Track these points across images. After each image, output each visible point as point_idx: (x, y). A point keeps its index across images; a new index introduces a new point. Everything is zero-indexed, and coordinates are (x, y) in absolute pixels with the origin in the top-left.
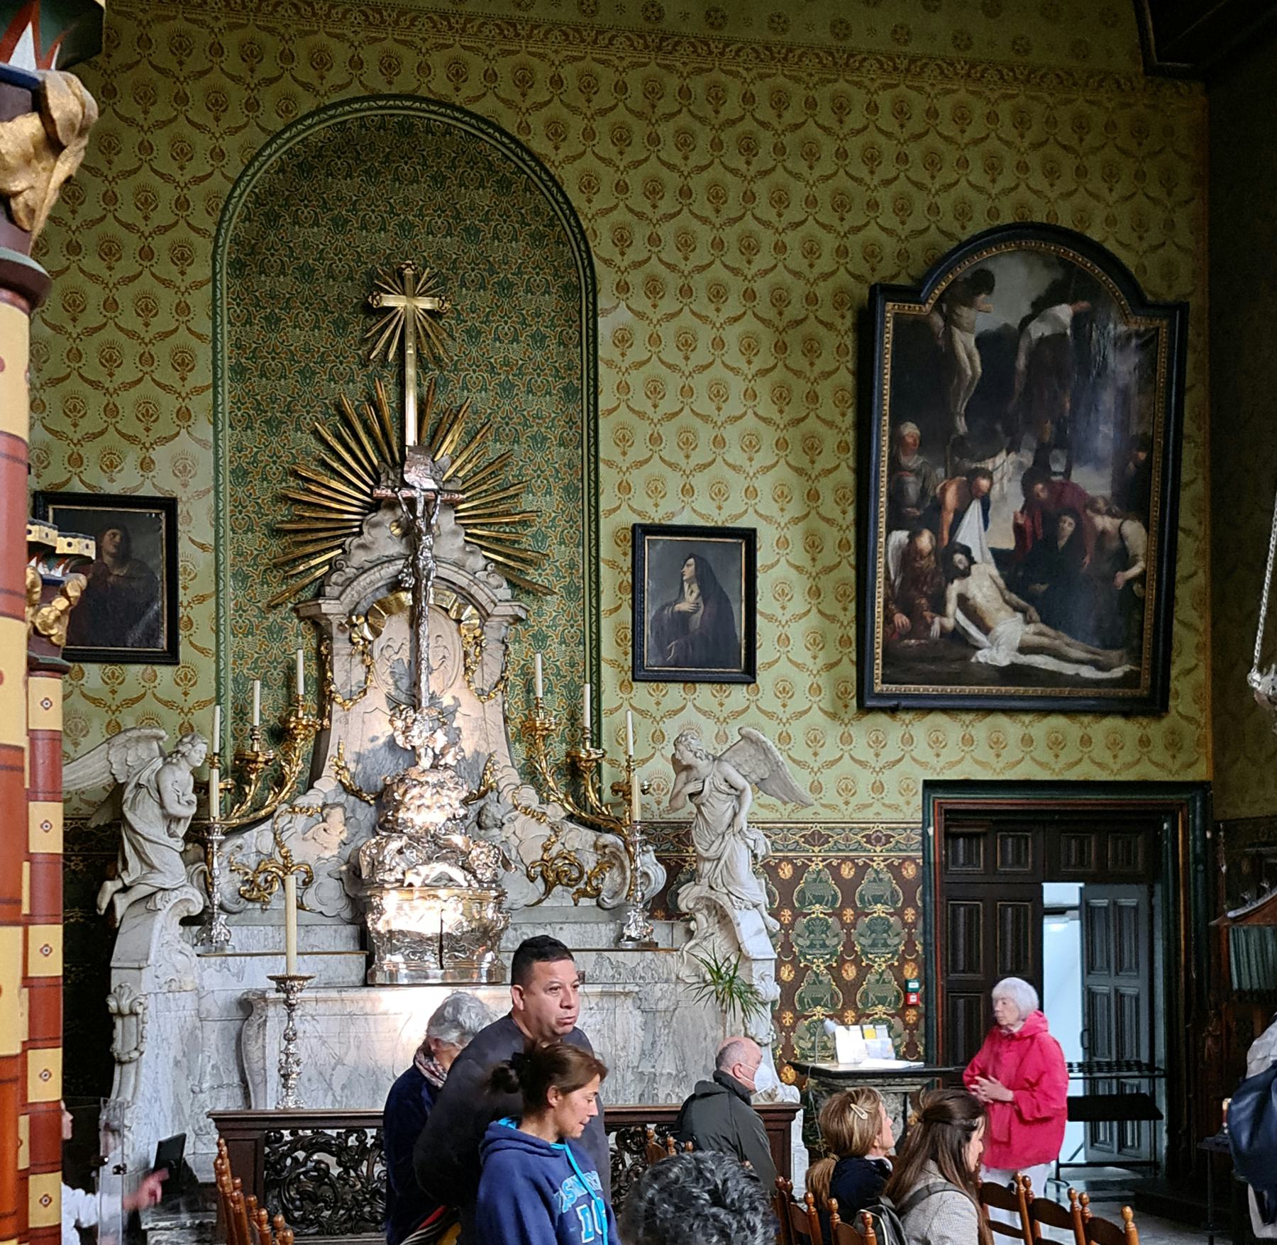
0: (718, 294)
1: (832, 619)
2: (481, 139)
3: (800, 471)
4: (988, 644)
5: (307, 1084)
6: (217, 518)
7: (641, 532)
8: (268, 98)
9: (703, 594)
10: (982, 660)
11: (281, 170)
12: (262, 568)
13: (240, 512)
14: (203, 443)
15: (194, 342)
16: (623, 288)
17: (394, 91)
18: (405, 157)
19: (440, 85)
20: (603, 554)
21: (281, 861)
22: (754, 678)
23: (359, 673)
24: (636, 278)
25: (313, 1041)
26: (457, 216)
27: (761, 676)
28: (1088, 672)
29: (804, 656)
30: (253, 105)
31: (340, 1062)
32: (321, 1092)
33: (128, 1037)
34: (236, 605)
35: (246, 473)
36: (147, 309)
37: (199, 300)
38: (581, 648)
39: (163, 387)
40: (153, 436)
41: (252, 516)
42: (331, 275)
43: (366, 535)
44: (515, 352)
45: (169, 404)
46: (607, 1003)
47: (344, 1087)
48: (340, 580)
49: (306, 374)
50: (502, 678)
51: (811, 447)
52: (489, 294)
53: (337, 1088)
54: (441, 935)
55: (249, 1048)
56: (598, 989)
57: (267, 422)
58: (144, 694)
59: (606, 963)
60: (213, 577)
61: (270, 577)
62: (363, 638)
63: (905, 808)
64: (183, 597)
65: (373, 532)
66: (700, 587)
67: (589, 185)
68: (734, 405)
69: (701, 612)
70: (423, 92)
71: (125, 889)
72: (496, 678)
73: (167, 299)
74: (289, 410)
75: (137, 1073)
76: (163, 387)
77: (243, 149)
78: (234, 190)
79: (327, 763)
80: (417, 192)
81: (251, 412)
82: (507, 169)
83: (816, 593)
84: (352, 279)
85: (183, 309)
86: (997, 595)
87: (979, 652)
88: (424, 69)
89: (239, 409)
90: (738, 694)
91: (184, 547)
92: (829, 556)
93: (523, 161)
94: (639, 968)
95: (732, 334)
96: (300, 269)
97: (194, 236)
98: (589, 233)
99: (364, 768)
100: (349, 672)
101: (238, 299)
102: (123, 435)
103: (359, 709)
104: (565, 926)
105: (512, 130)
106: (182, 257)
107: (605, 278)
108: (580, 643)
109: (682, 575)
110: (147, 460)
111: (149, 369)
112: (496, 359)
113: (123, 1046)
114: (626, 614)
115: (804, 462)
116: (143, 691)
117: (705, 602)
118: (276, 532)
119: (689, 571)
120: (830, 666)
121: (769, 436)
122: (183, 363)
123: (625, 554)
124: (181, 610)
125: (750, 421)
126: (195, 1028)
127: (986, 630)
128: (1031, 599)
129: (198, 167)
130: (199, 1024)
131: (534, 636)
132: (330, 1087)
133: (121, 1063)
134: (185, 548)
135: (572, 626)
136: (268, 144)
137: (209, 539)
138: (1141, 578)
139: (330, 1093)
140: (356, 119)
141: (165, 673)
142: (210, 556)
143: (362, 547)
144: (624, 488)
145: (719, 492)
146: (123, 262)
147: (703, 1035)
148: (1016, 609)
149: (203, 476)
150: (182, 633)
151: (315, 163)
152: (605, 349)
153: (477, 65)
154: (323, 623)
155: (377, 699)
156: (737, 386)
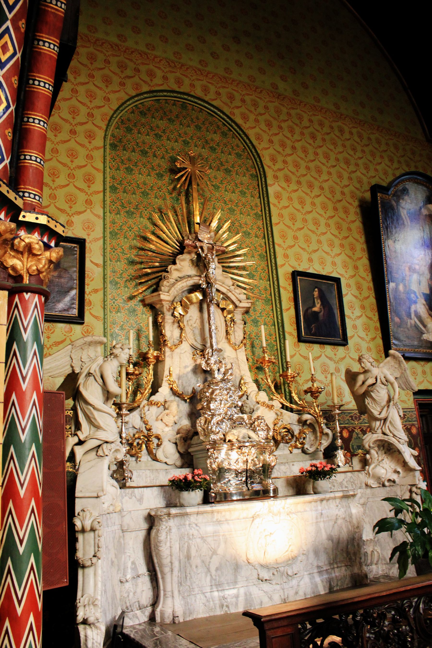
0: (311, 186)
1: (370, 318)
2: (214, 116)
3: (349, 257)
4: (426, 332)
5: (195, 569)
6: (104, 252)
7: (295, 274)
8: (129, 83)
9: (322, 304)
10: (425, 338)
11: (133, 112)
12: (125, 279)
13: (114, 252)
14: (98, 216)
15: (94, 172)
16: (276, 177)
17: (181, 90)
18: (185, 117)
19: (199, 92)
20: (281, 284)
21: (146, 432)
22: (347, 342)
23: (177, 332)
24: (280, 174)
25: (199, 540)
26: (207, 142)
27: (350, 342)
29: (363, 334)
30: (122, 84)
31: (215, 553)
32: (203, 575)
33: (87, 548)
34: (112, 296)
35: (116, 234)
36: (73, 155)
37: (98, 155)
38: (273, 327)
39: (79, 189)
40: (73, 210)
41: (120, 254)
42: (155, 156)
43: (178, 264)
44: (234, 197)
45: (81, 197)
46: (345, 502)
47: (217, 569)
48: (168, 284)
49: (145, 194)
50: (244, 338)
51: (353, 249)
52: (222, 173)
53: (213, 569)
54: (247, 470)
55: (161, 549)
56: (341, 494)
57: (127, 212)
58: (65, 339)
60: (102, 281)
61: (128, 284)
62: (180, 314)
63: (408, 402)
64: (87, 290)
65: (182, 263)
66: (321, 301)
67: (259, 138)
68: (323, 229)
69: (323, 312)
70: (192, 93)
72: (242, 338)
73: (82, 152)
74: (137, 208)
75: (95, 574)
76: (79, 189)
77: (118, 99)
78: (113, 114)
79: (165, 379)
80: (190, 130)
81: (119, 207)
82: (225, 129)
83: (363, 307)
84: (164, 158)
85: (89, 157)
86: (426, 312)
87: (424, 335)
88: (192, 86)
89: (114, 205)
90: (341, 349)
91: (88, 265)
92: (366, 293)
93: (232, 126)
94: (344, 482)
95: (318, 201)
96: (141, 151)
97: (96, 129)
98: (261, 155)
99: (182, 383)
100: (172, 331)
101: (113, 159)
102: (58, 209)
103: (177, 351)
104: (295, 463)
105: (228, 113)
106: (90, 136)
107: (270, 174)
108: (272, 325)
109: (314, 295)
110: (70, 221)
111: (72, 181)
112: (227, 198)
113: (84, 555)
114: (292, 311)
115: (350, 254)
116: (65, 337)
117: (324, 309)
118: (132, 263)
119: (316, 293)
120: (373, 339)
121: (337, 242)
122: (89, 180)
123: (289, 285)
124: (86, 296)
125: (329, 235)
126: (120, 537)
127: (425, 326)
129: (98, 102)
130: (121, 534)
131: (253, 321)
132: (209, 570)
133: (84, 567)
135: (268, 317)
136: (128, 100)
137: (101, 262)
139: (209, 575)
140: (164, 99)
141: (77, 328)
142: (101, 270)
143: (177, 270)
144: (286, 256)
145: (322, 263)
146: (61, 134)
149: (98, 231)
150: (86, 308)
151: (147, 112)
152: (272, 199)
153: (213, 89)
154: (158, 306)
155: (185, 347)
156: (323, 221)
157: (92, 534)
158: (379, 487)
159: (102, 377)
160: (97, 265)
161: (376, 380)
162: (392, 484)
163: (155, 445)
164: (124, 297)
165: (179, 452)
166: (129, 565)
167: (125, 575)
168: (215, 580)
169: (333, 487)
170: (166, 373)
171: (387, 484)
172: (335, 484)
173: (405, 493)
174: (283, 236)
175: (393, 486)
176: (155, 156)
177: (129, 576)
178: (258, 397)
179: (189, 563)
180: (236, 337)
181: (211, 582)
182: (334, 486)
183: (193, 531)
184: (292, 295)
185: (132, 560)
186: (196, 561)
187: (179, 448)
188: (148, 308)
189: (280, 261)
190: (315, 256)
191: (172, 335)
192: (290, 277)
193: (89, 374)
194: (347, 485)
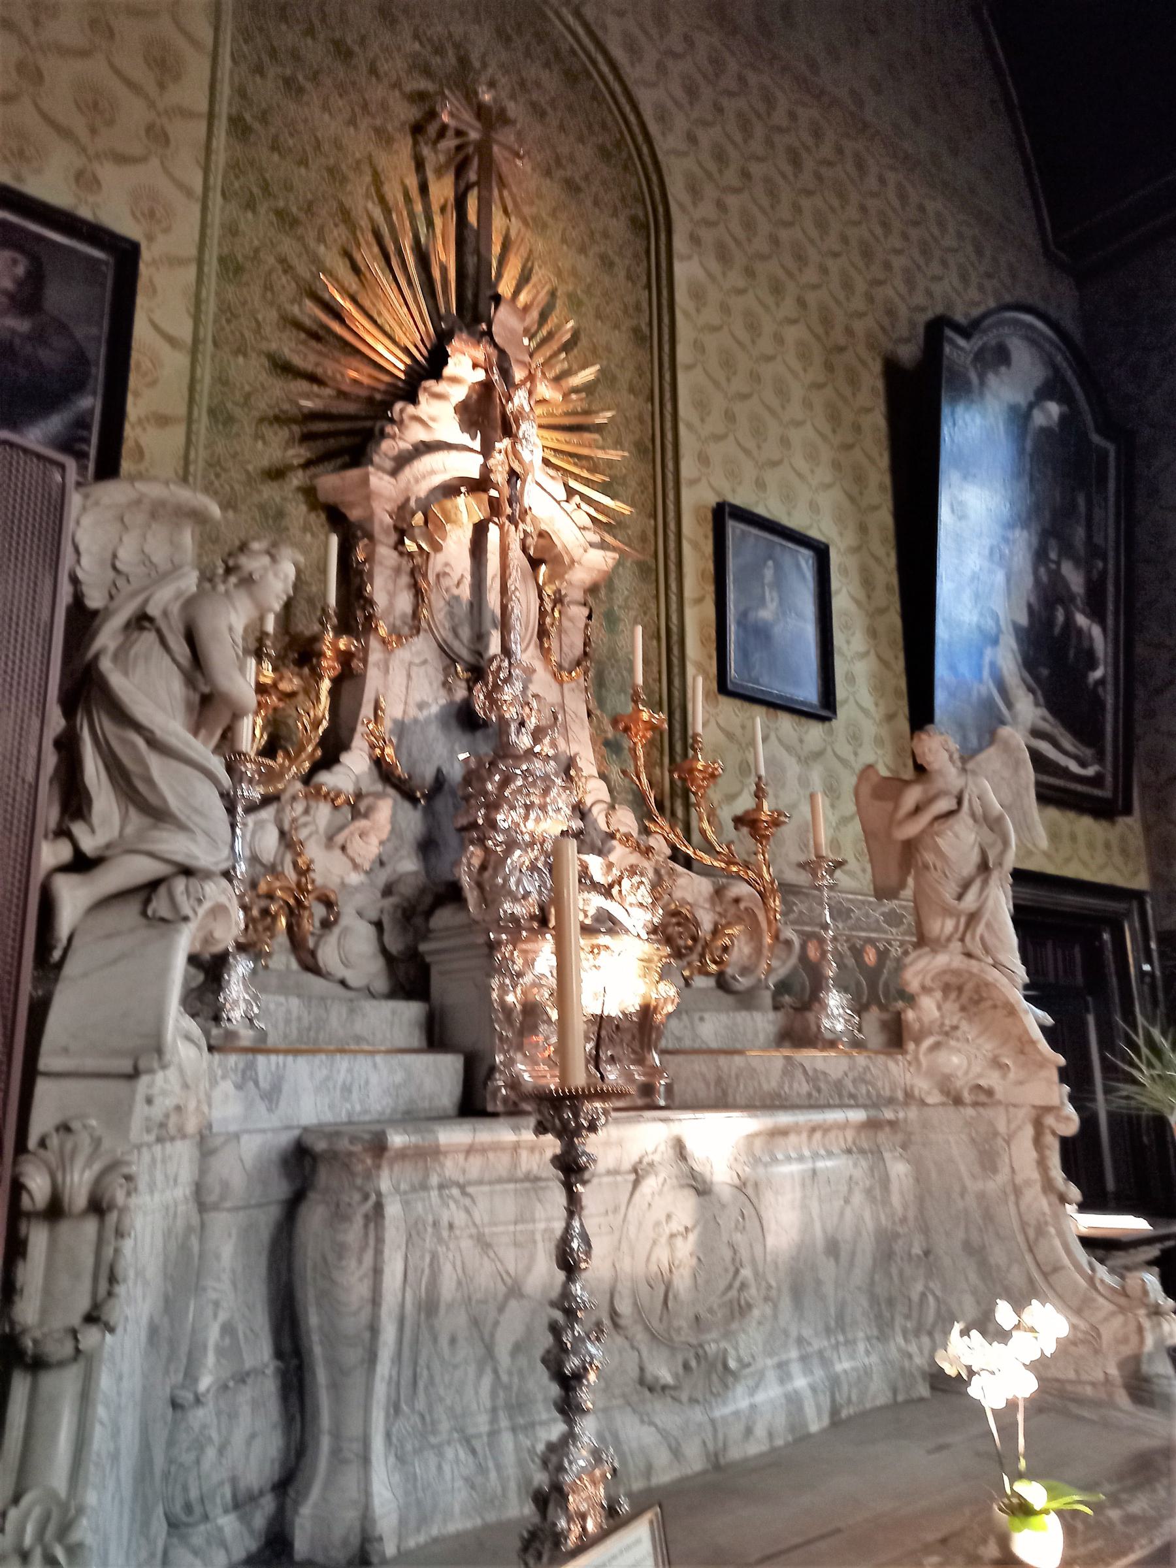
3: (852, 499)
22: (835, 712)
28: (1074, 767)
32: (472, 1370)
38: (655, 643)
50: (585, 653)
51: (860, 479)
59: (799, 1074)
64: (134, 409)
71: (82, 864)
79: (360, 729)
83: (872, 633)
113: (44, 1312)
114: (709, 609)
123: (706, 537)
126: (189, 1229)
127: (1009, 705)
128: (1036, 678)
133: (38, 1365)
134: (141, 330)
138: (1102, 682)
147: (957, 1188)
148: (1030, 690)
154: (354, 514)
157: (90, 1227)
158: (943, 1104)
159: (191, 638)
160: (172, 341)
161: (960, 802)
162: (983, 1098)
163: (317, 924)
164: (250, 468)
165: (384, 951)
166: (213, 1333)
167: (191, 1376)
168: (507, 1388)
169: (815, 1094)
170: (367, 711)
171: (967, 1097)
172: (823, 1086)
173: (1020, 1128)
174: (702, 406)
175: (983, 1105)
176: (373, 71)
177: (205, 1382)
178: (612, 821)
179: (431, 1328)
180: (565, 649)
181: (494, 1394)
182: (819, 1090)
183: (454, 1213)
184: (710, 566)
185: (223, 1316)
186: (453, 1321)
187: (387, 938)
188: (323, 516)
189: (688, 468)
190: (771, 476)
191: (391, 605)
192: (710, 516)
193: (141, 621)
194: (853, 1090)
